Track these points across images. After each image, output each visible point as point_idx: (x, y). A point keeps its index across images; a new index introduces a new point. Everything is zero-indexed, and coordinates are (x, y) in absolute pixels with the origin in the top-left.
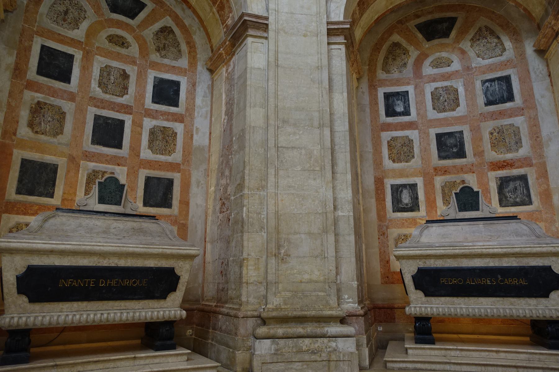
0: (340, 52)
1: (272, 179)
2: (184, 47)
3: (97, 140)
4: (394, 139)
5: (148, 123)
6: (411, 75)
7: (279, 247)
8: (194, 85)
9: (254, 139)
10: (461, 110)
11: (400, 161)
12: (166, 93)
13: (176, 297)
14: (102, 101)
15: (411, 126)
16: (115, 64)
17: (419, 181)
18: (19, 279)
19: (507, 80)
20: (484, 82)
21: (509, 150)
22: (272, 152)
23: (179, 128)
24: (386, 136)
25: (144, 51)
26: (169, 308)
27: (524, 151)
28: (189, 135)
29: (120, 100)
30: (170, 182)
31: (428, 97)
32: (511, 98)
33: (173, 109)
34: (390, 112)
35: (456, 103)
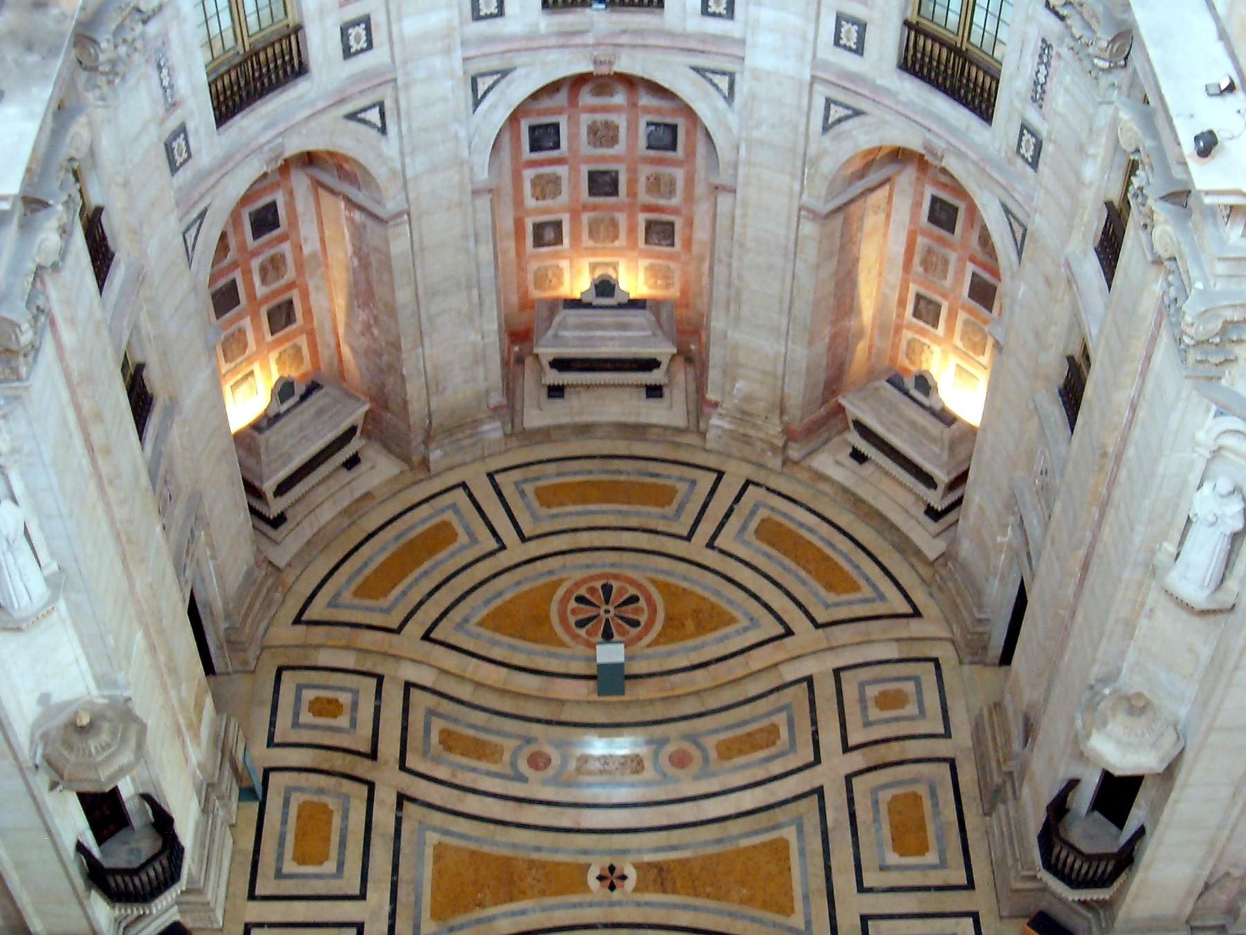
4: (539, 177)
5: (255, 264)
6: (566, 104)
7: (437, 386)
8: (291, 193)
9: (405, 316)
10: (620, 148)
11: (544, 198)
15: (560, 161)
17: (566, 219)
19: (673, 129)
20: (649, 124)
21: (662, 197)
24: (528, 174)
27: (675, 201)
28: (298, 248)
31: (584, 131)
32: (673, 147)
35: (614, 140)
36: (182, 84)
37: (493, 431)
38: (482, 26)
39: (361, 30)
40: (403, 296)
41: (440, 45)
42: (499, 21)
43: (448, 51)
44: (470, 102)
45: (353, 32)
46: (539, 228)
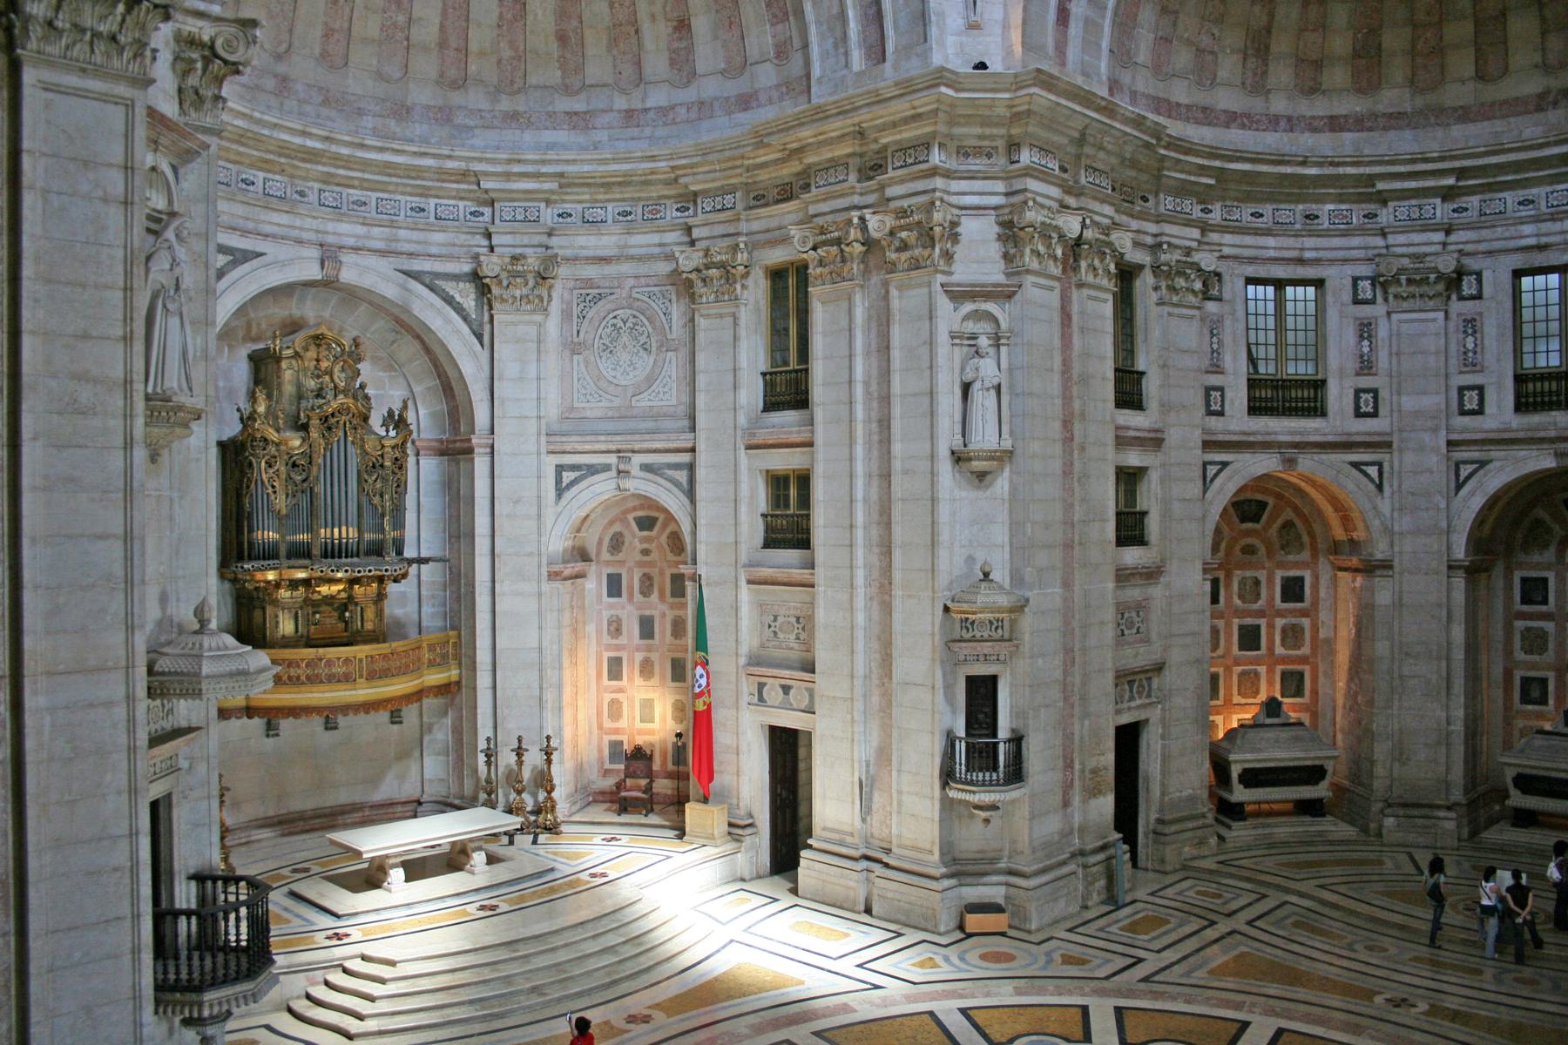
0: (1459, 583)
1: (1396, 703)
2: (1306, 539)
3: (1243, 646)
4: (1528, 629)
5: (1280, 622)
12: (1293, 590)
13: (1324, 784)
14: (1244, 611)
15: (1547, 617)
16: (1248, 574)
17: (1551, 676)
18: (1240, 776)
22: (1397, 682)
23: (1306, 622)
24: (1520, 624)
25: (1270, 553)
26: (1321, 791)
28: (1315, 629)
29: (1255, 606)
30: (1301, 675)
33: (1299, 605)
34: (1526, 600)
36: (1228, 361)
37: (1449, 824)
38: (1466, 420)
39: (1369, 396)
40: (1382, 648)
41: (1429, 424)
42: (1480, 417)
43: (1435, 430)
44: (1453, 485)
45: (1364, 396)
46: (1526, 682)
